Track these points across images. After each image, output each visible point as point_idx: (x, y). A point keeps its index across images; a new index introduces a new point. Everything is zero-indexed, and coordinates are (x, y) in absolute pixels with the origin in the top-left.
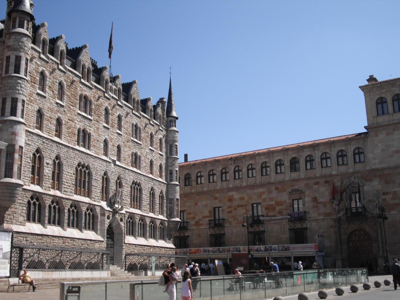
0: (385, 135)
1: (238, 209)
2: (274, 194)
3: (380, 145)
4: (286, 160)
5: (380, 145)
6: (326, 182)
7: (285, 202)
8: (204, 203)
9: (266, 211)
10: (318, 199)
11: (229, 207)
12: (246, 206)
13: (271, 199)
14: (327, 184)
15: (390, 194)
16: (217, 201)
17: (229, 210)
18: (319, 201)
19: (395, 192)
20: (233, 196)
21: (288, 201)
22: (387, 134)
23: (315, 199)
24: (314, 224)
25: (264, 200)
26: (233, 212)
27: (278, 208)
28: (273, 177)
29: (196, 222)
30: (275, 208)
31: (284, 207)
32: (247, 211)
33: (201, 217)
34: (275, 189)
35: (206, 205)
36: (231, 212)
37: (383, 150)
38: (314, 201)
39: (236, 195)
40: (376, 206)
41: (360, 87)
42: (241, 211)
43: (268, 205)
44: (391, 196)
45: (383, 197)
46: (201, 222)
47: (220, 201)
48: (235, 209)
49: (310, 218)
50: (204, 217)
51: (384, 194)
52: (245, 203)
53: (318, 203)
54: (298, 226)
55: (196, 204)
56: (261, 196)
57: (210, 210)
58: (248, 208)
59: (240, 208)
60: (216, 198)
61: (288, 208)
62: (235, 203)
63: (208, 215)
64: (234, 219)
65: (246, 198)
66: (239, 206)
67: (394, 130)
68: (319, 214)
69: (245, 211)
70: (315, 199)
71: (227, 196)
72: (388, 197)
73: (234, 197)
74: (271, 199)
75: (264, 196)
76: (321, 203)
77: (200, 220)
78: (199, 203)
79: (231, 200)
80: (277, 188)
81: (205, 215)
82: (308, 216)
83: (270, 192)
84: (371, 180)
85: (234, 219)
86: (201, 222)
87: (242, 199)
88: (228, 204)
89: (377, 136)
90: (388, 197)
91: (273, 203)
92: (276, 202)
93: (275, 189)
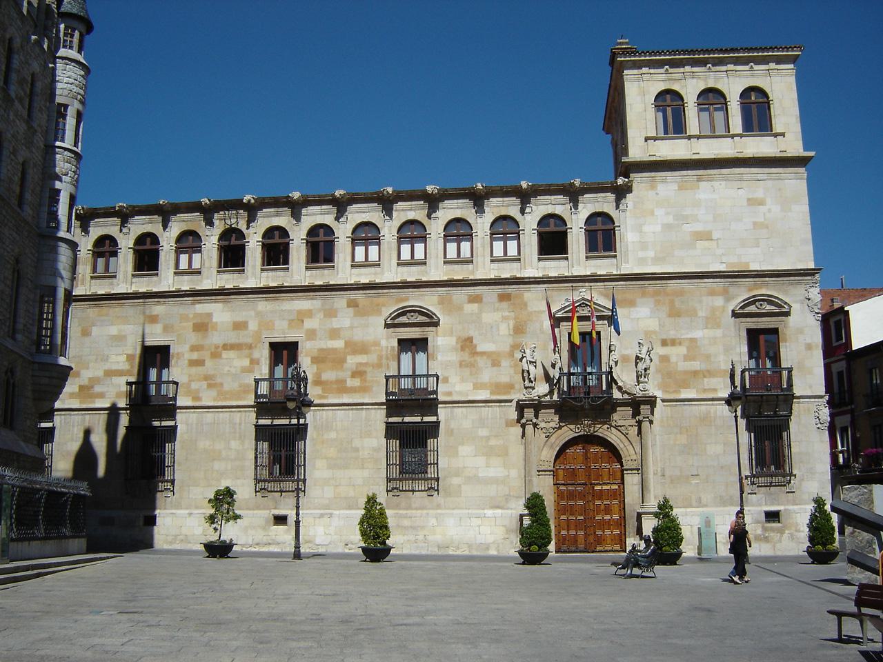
0: (675, 187)
1: (225, 354)
2: (344, 319)
3: (659, 212)
5: (659, 212)
6: (503, 298)
7: (377, 344)
8: (114, 330)
9: (315, 367)
10: (474, 341)
11: (194, 348)
12: (250, 347)
13: (334, 334)
14: (505, 304)
15: (680, 344)
17: (195, 356)
18: (479, 349)
19: (693, 340)
20: (210, 315)
21: (384, 343)
22: (681, 188)
23: (467, 344)
24: (459, 411)
25: (312, 334)
26: (209, 363)
27: (352, 361)
28: (342, 272)
29: (81, 388)
30: (343, 360)
31: (371, 358)
33: (100, 373)
34: (349, 306)
35: (120, 339)
36: (199, 363)
37: (667, 227)
38: (463, 349)
39: (219, 312)
42: (236, 361)
43: (321, 350)
46: (98, 389)
47: (166, 329)
48: (215, 355)
49: (450, 394)
50: (110, 373)
51: (664, 343)
52: (249, 340)
53: (474, 353)
56: (303, 321)
57: (130, 352)
58: (256, 355)
61: (384, 361)
62: (216, 339)
63: (126, 367)
64: (210, 386)
65: (253, 326)
66: (227, 347)
67: (699, 179)
68: (477, 386)
69: (246, 362)
70: (467, 344)
71: (191, 316)
72: (676, 353)
73: (214, 320)
74: (334, 334)
75: (309, 324)
76: (483, 353)
77: (94, 381)
78: (95, 331)
79: (202, 326)
80: (352, 304)
81: (114, 367)
82: (442, 388)
83: (331, 313)
85: (210, 386)
86: (98, 389)
87: (240, 326)
88: (193, 338)
89: (653, 187)
90: (676, 353)
91: (339, 344)
92: (346, 343)
93: (349, 306)
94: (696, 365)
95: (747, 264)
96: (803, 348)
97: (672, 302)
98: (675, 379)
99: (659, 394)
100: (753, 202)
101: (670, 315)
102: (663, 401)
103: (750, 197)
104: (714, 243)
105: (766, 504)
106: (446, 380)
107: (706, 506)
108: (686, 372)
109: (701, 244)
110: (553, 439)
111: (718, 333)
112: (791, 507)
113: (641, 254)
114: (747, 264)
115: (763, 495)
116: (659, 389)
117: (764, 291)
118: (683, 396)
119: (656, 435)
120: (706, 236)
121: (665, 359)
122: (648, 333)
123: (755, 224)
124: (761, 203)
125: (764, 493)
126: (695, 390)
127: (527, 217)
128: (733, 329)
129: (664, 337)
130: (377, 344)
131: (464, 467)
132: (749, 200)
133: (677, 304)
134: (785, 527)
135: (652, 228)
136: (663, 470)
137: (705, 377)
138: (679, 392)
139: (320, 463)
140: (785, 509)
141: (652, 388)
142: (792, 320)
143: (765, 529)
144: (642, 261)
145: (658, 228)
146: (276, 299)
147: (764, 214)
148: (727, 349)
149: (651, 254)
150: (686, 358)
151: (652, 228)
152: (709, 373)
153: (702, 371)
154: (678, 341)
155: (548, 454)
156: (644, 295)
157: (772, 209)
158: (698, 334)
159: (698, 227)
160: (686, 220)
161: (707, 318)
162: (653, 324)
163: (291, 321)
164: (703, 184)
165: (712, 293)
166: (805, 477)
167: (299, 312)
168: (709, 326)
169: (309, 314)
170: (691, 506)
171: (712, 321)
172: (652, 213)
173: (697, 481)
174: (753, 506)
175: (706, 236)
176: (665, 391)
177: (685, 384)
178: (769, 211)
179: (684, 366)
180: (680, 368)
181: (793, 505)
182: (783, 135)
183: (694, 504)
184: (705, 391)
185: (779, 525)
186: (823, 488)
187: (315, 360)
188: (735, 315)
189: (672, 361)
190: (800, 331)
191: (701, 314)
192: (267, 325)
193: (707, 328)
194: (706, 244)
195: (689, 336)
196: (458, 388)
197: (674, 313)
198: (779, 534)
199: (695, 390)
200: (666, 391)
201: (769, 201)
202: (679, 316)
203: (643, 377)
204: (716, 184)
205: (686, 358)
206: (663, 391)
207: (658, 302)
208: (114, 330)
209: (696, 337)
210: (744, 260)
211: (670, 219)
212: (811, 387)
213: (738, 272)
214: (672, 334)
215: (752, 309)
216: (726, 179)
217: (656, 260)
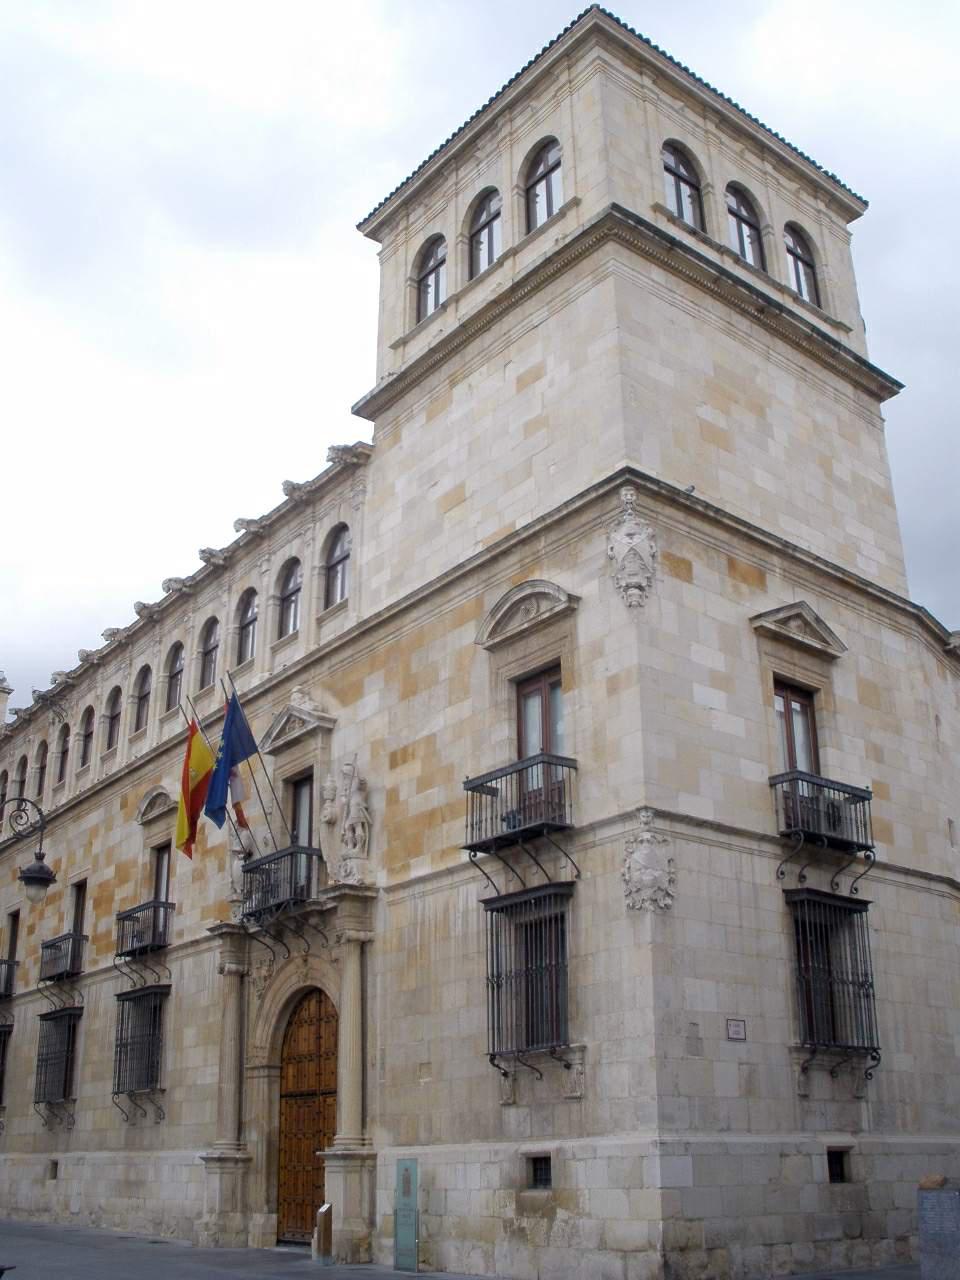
0: (422, 419)
3: (400, 485)
4: (156, 661)
7: (135, 862)
19: (431, 739)
32: (61, 919)
37: (410, 506)
40: (349, 834)
41: (359, 227)
44: (414, 769)
48: (41, 916)
49: (181, 934)
54: (151, 980)
67: (453, 384)
75: (96, 848)
83: (108, 824)
94: (436, 796)
95: (513, 524)
96: (602, 692)
99: (382, 879)
100: (523, 383)
102: (390, 890)
103: (522, 370)
105: (531, 1138)
107: (438, 1141)
110: (267, 1005)
111: (465, 708)
112: (571, 1144)
114: (513, 524)
115: (527, 1110)
116: (383, 868)
118: (415, 874)
119: (376, 976)
120: (457, 498)
121: (393, 796)
122: (376, 746)
123: (529, 428)
125: (529, 1106)
127: (266, 579)
128: (487, 692)
129: (394, 747)
130: (135, 862)
131: (188, 1069)
133: (414, 668)
137: (443, 821)
138: (406, 867)
139: (88, 1070)
140: (559, 1150)
142: (587, 626)
143: (522, 1208)
146: (79, 817)
147: (543, 394)
149: (386, 575)
150: (424, 783)
151: (392, 520)
153: (441, 808)
154: (410, 750)
155: (261, 1035)
156: (373, 668)
159: (446, 484)
160: (430, 479)
161: (451, 679)
163: (85, 846)
164: (459, 390)
165: (460, 621)
171: (459, 689)
173: (427, 1080)
174: (509, 1139)
176: (391, 871)
177: (414, 849)
178: (551, 385)
181: (581, 1136)
183: (423, 1135)
184: (444, 854)
188: (490, 649)
189: (403, 796)
191: (444, 674)
193: (450, 704)
195: (425, 733)
201: (551, 362)
202: (414, 693)
203: (350, 846)
204: (474, 378)
205: (424, 783)
206: (388, 871)
209: (434, 730)
210: (507, 521)
213: (488, 550)
215: (517, 625)
216: (487, 357)
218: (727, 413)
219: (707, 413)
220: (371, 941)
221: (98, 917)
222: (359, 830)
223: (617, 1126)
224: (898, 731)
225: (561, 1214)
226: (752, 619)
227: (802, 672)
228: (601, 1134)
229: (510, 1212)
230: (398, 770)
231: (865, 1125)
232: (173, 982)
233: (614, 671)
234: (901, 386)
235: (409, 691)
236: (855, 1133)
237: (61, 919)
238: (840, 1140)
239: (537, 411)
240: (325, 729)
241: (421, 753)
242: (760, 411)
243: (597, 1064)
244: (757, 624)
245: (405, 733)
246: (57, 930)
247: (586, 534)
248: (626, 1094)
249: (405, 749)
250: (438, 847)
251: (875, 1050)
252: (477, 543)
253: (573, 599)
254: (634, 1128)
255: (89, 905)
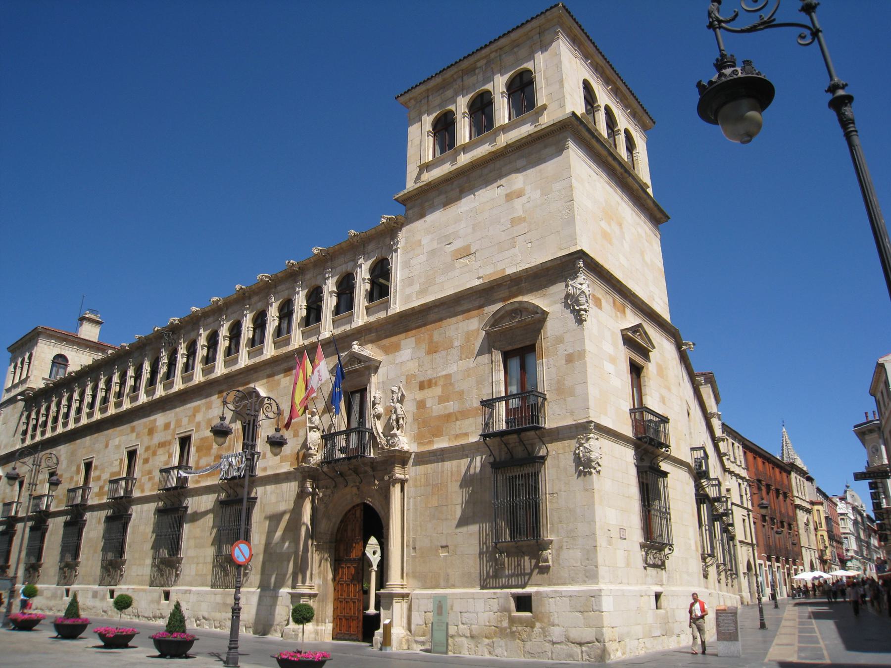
15: (436, 384)
16: (134, 434)
17: (146, 456)
19: (448, 376)
25: (198, 425)
35: (118, 447)
37: (433, 253)
39: (160, 419)
43: (202, 439)
44: (438, 391)
45: (419, 395)
48: (154, 454)
49: (265, 469)
51: (422, 386)
55: (107, 446)
59: (160, 451)
60: (133, 430)
62: (158, 438)
64: (150, 479)
65: (172, 426)
66: (162, 445)
84: (397, 348)
87: (167, 426)
88: (146, 441)
94: (452, 406)
97: (431, 337)
98: (429, 426)
100: (509, 197)
101: (429, 352)
103: (508, 191)
104: (472, 257)
106: (264, 457)
107: (453, 586)
108: (440, 417)
109: (459, 264)
113: (408, 291)
117: (520, 299)
120: (466, 253)
122: (409, 378)
123: (514, 222)
124: (519, 194)
126: (447, 438)
129: (422, 379)
132: (507, 195)
133: (436, 337)
134: (536, 618)
135: (419, 261)
136: (414, 540)
137: (457, 419)
138: (431, 442)
140: (537, 592)
141: (405, 442)
142: (551, 328)
143: (512, 621)
144: (408, 298)
145: (424, 258)
148: (479, 383)
149: (417, 287)
150: (442, 399)
152: (463, 414)
154: (434, 381)
157: (533, 194)
158: (452, 369)
159: (458, 244)
161: (462, 347)
162: (412, 367)
163: (190, 416)
166: (565, 544)
167: (194, 408)
168: (463, 357)
169: (196, 410)
170: (437, 586)
172: (420, 241)
175: (466, 253)
176: (420, 444)
177: (437, 433)
179: (436, 409)
180: (435, 414)
181: (549, 585)
182: (544, 107)
183: (442, 584)
184: (457, 436)
185: (528, 614)
186: (588, 559)
187: (198, 450)
190: (559, 340)
191: (456, 344)
192: (179, 423)
193: (461, 359)
194: (465, 260)
195: (444, 373)
196: (270, 463)
197: (433, 350)
198: (527, 629)
199: (447, 438)
200: (422, 443)
201: (528, 189)
203: (395, 429)
205: (442, 399)
207: (418, 342)
208: (116, 441)
210: (500, 267)
211: (435, 245)
212: (572, 413)
214: (430, 374)
217: (422, 292)
218: (609, 224)
219: (603, 224)
220: (407, 480)
221: (199, 458)
222: (401, 421)
223: (572, 581)
224: (669, 389)
225: (538, 625)
226: (622, 331)
227: (639, 360)
228: (564, 584)
229: (505, 624)
230: (425, 391)
231: (665, 582)
232: (259, 495)
233: (571, 351)
234: (669, 218)
235: (433, 350)
236: (661, 585)
237: (170, 456)
238: (658, 589)
239: (520, 213)
240: (372, 367)
241: (441, 383)
242: (620, 225)
243: (561, 548)
244: (625, 333)
245: (430, 372)
246: (167, 463)
247: (553, 282)
248: (579, 564)
249: (430, 381)
250: (453, 432)
251: (671, 545)
252: (479, 278)
253: (545, 314)
254: (585, 582)
255: (193, 450)
